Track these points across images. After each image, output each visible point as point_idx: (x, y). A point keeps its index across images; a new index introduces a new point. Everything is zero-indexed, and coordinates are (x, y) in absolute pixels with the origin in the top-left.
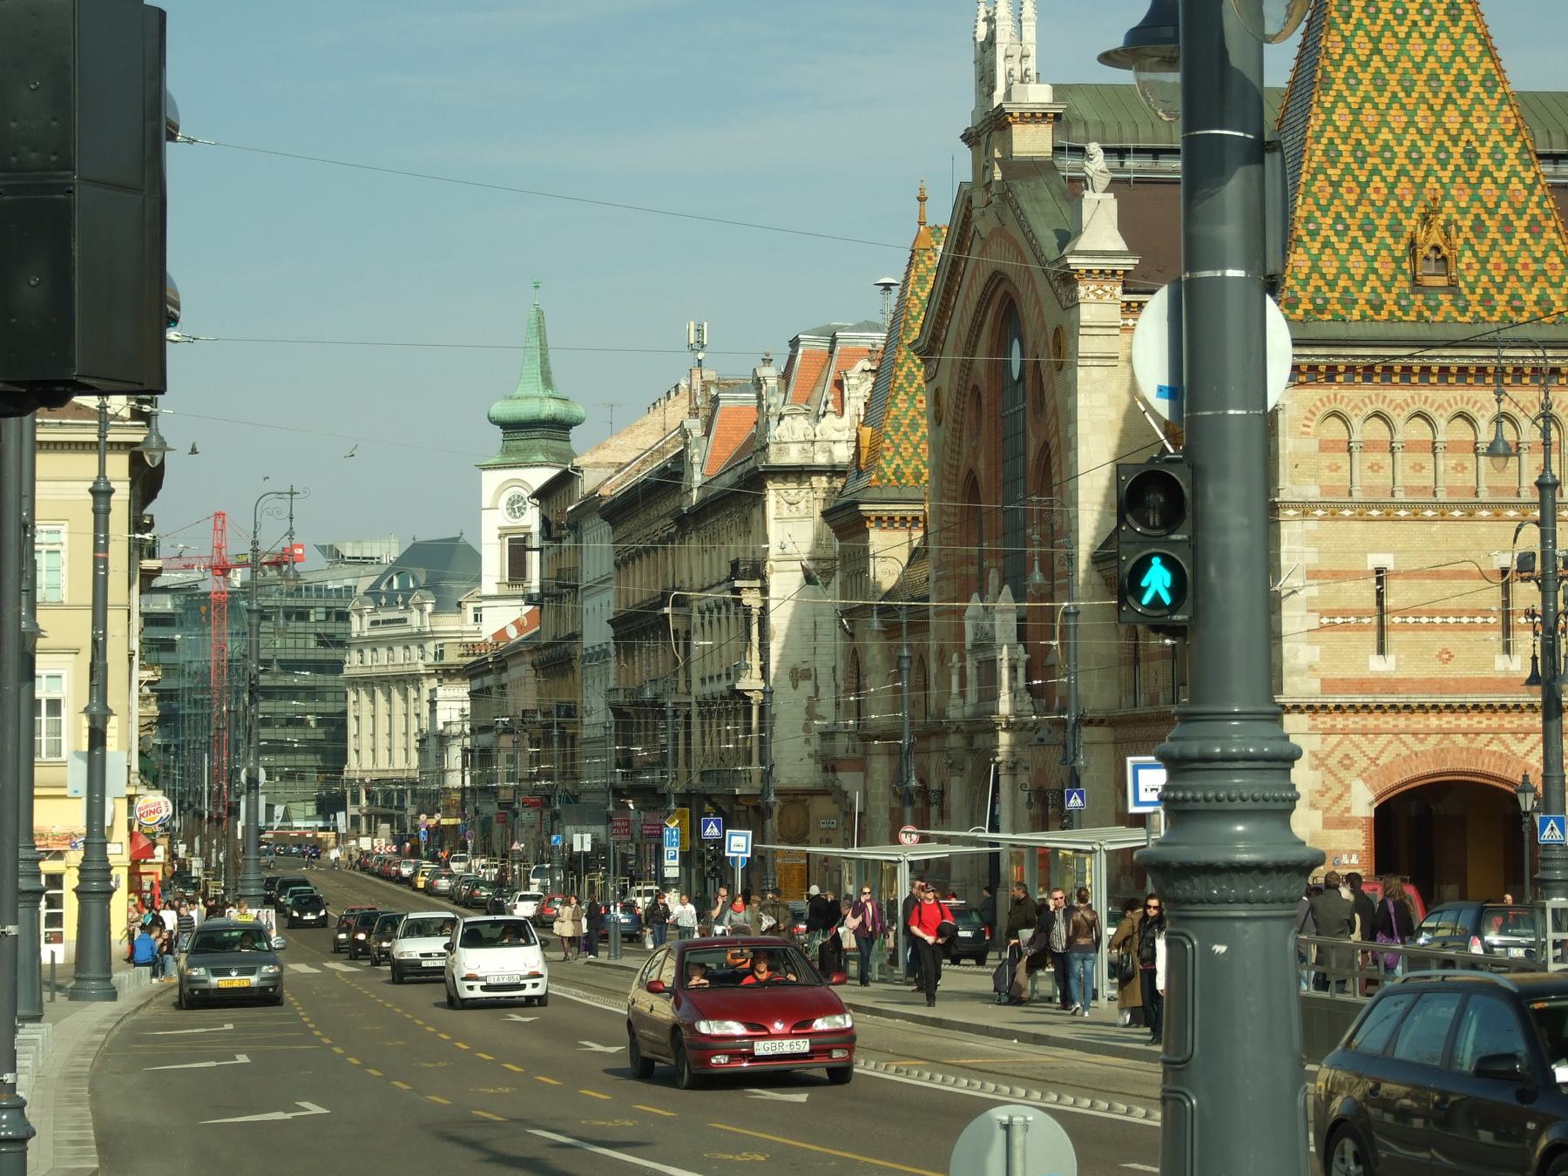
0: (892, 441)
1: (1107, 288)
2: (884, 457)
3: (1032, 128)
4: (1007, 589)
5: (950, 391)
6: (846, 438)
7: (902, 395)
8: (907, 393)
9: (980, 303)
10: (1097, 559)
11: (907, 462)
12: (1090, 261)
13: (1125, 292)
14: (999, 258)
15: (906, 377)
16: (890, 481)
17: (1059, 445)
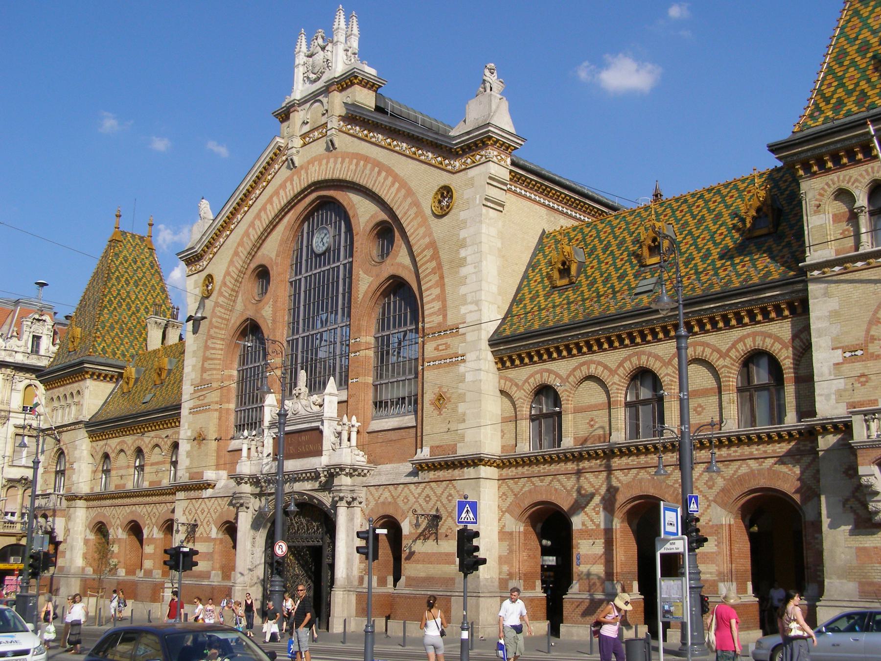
0: (101, 333)
1: (503, 157)
2: (97, 341)
3: (365, 91)
4: (332, 378)
5: (228, 273)
6: (22, 350)
7: (106, 311)
8: (108, 310)
9: (282, 209)
10: (494, 342)
11: (109, 346)
12: (500, 133)
13: (513, 163)
14: (317, 174)
15: (108, 302)
16: (100, 354)
17: (439, 266)
